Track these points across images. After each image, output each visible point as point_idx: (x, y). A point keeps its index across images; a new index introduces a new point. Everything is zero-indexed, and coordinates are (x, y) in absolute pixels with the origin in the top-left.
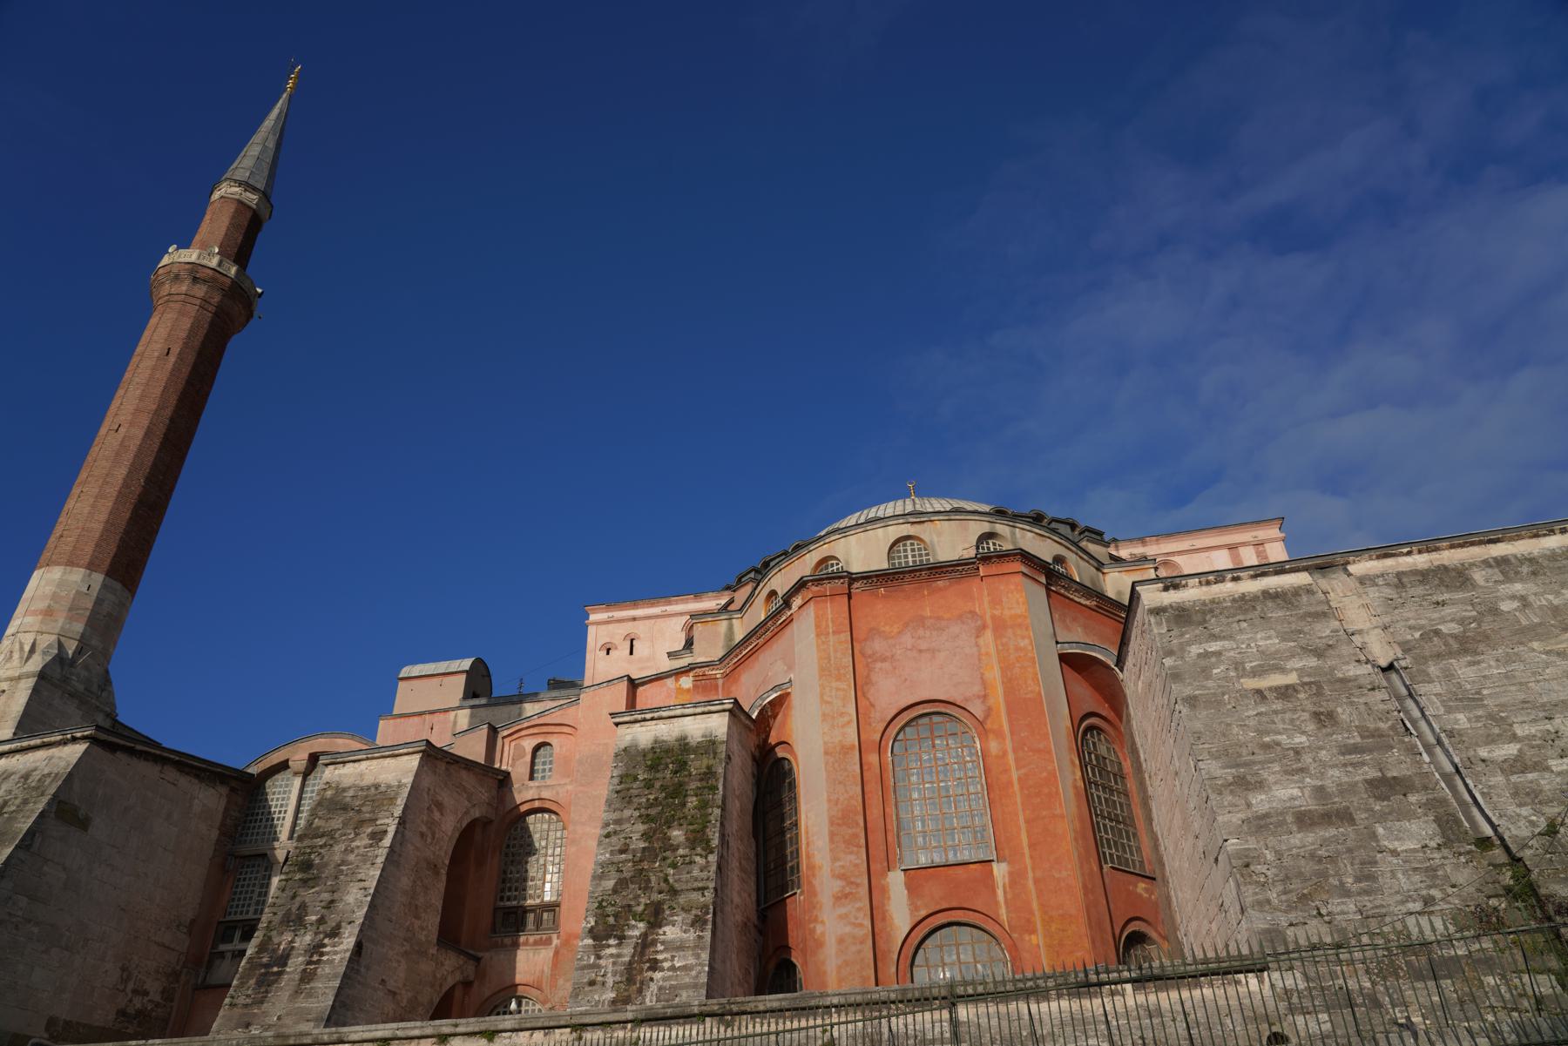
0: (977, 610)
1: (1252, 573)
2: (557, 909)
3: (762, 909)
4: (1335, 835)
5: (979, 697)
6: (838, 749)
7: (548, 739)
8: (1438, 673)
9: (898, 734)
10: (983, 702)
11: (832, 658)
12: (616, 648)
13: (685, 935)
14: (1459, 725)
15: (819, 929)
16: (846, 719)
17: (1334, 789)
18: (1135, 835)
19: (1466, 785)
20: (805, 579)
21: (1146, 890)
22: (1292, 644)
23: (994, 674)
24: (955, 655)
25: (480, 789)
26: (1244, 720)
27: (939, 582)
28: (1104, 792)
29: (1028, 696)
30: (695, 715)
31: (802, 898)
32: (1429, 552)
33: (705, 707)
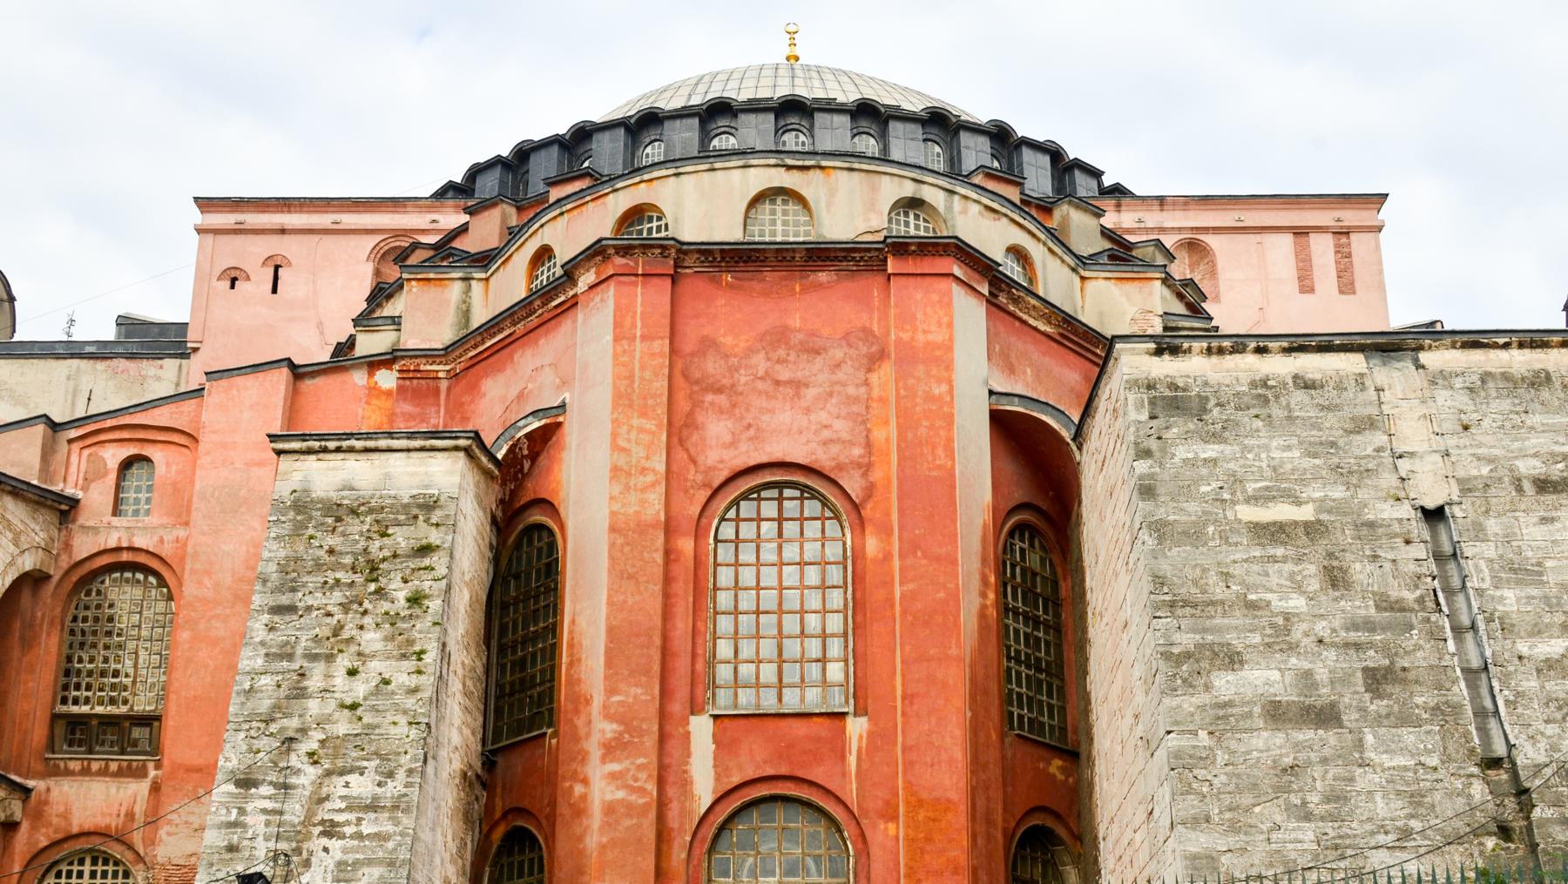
0: (875, 328)
1: (1285, 344)
2: (156, 724)
3: (490, 751)
4: (1310, 739)
5: (860, 466)
6: (632, 525)
7: (148, 451)
8: (1497, 529)
9: (728, 509)
10: (865, 475)
11: (637, 378)
12: (248, 278)
13: (379, 790)
14: (1504, 605)
15: (578, 789)
16: (650, 478)
17: (1324, 677)
18: (1061, 690)
19: (1491, 688)
20: (604, 242)
21: (1062, 769)
22: (1317, 461)
23: (886, 434)
24: (831, 395)
25: (32, 526)
26: (1227, 566)
27: (820, 274)
28: (1026, 624)
29: (934, 473)
30: (409, 450)
31: (554, 741)
32: (1532, 347)
33: (431, 439)
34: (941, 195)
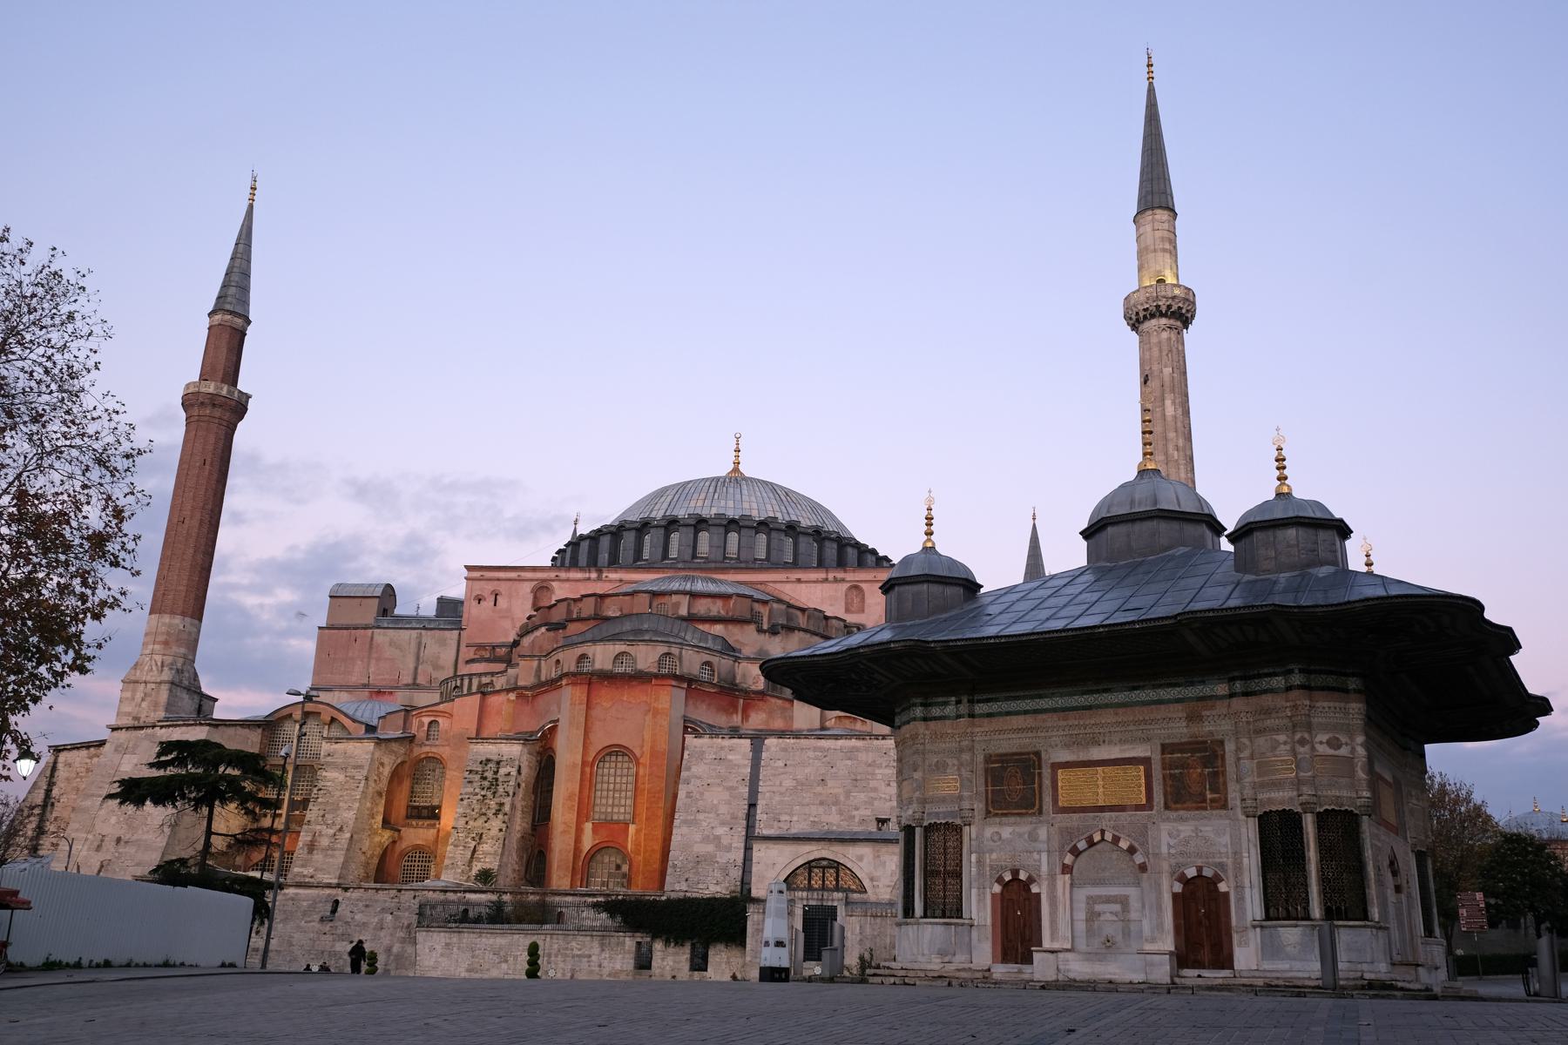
12: (485, 600)
23: (647, 736)
34: (679, 650)
